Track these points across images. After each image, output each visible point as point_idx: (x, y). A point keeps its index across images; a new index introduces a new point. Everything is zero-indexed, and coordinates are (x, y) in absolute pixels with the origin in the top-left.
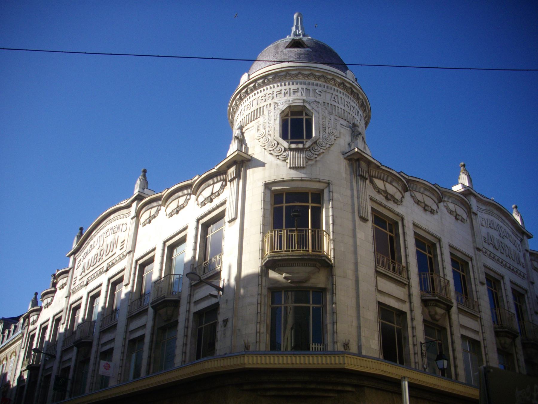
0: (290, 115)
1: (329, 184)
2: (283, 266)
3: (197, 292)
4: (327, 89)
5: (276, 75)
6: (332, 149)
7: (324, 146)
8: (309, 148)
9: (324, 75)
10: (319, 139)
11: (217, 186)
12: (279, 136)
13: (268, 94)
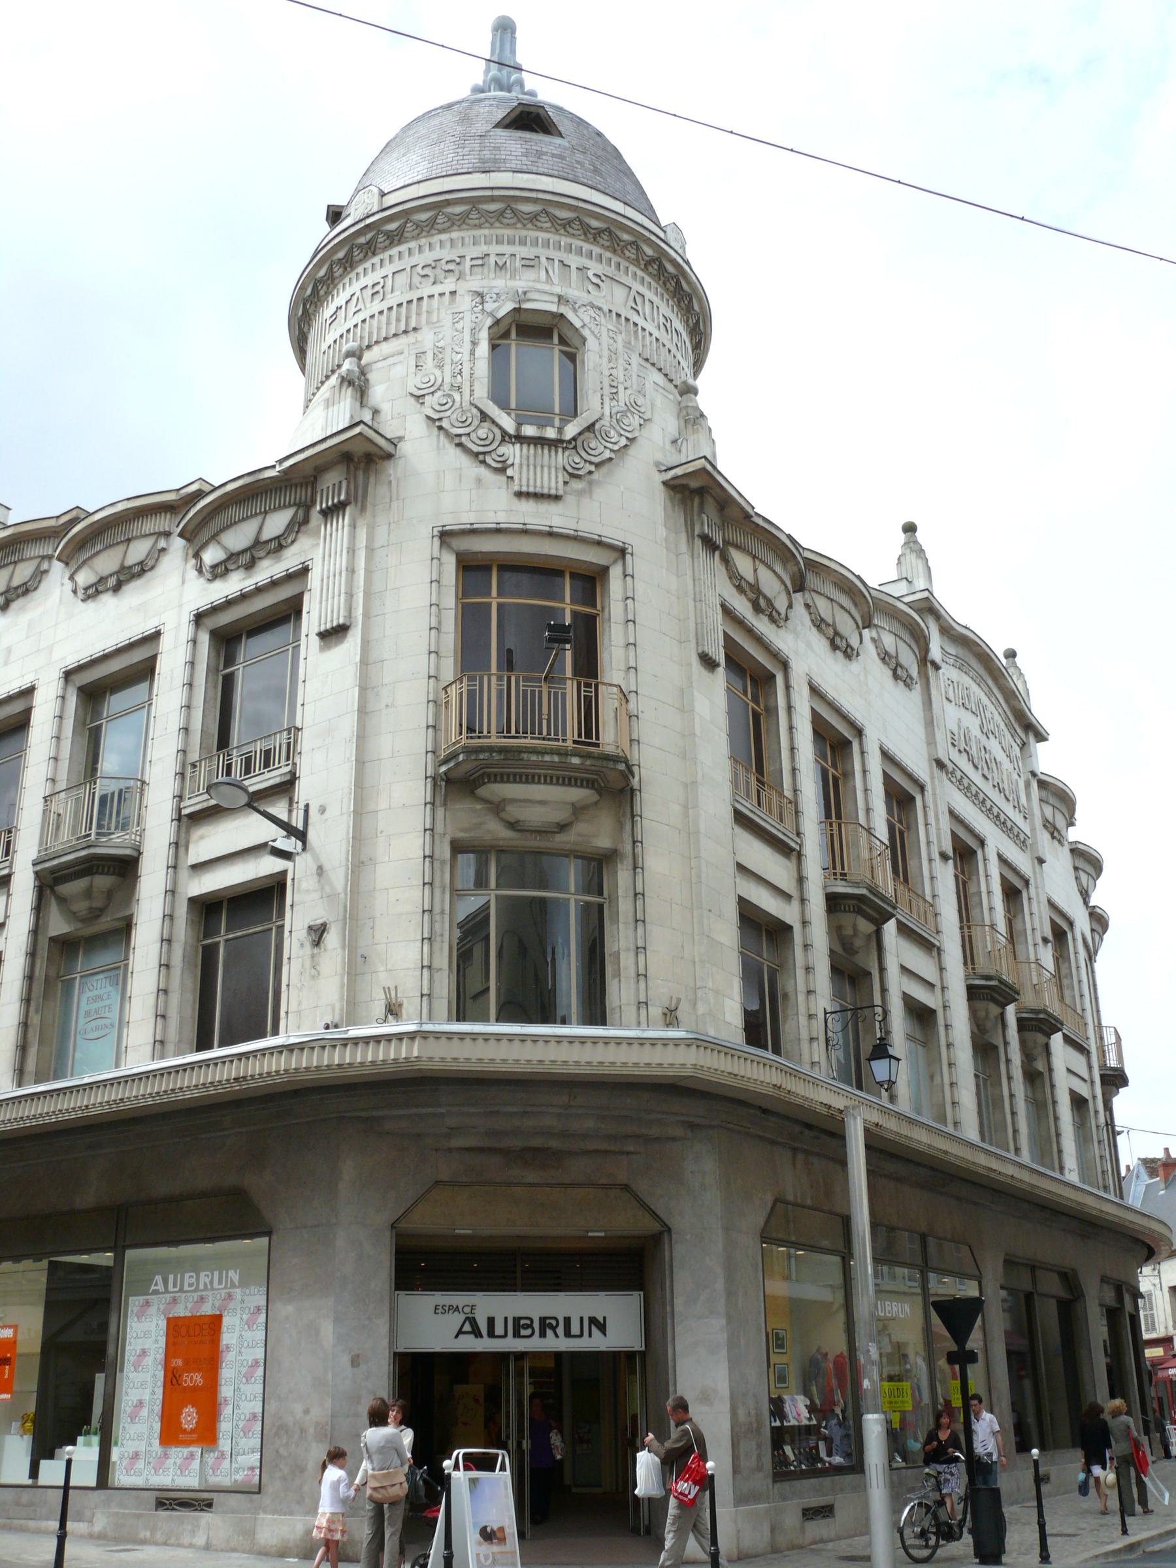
1: (622, 552)
3: (202, 838)
4: (616, 272)
6: (632, 451)
7: (612, 440)
8: (573, 443)
11: (276, 523)
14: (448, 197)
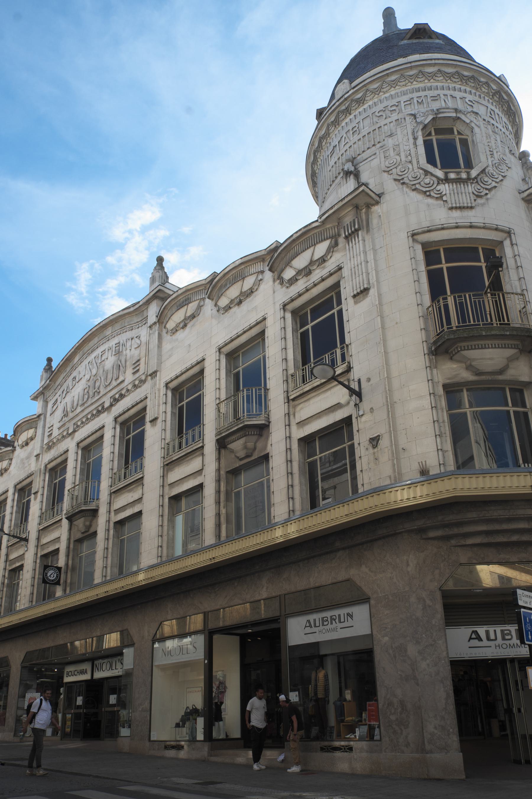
0: (433, 133)
1: (509, 233)
2: (468, 349)
3: (302, 409)
4: (479, 99)
5: (402, 75)
6: (505, 183)
7: (496, 177)
8: (476, 180)
9: (476, 75)
10: (487, 166)
11: (321, 249)
12: (426, 162)
13: (377, 112)
14: (387, 72)
